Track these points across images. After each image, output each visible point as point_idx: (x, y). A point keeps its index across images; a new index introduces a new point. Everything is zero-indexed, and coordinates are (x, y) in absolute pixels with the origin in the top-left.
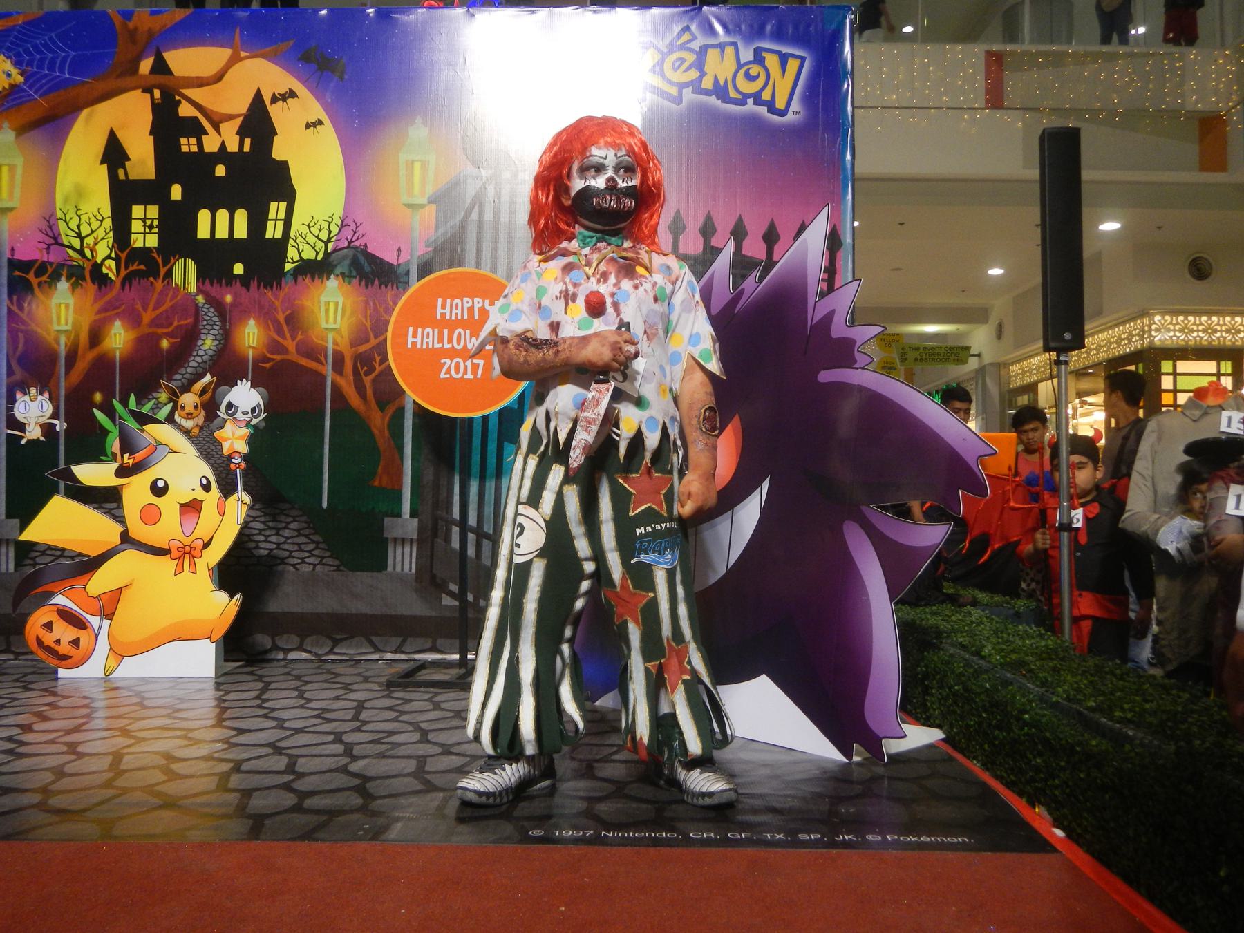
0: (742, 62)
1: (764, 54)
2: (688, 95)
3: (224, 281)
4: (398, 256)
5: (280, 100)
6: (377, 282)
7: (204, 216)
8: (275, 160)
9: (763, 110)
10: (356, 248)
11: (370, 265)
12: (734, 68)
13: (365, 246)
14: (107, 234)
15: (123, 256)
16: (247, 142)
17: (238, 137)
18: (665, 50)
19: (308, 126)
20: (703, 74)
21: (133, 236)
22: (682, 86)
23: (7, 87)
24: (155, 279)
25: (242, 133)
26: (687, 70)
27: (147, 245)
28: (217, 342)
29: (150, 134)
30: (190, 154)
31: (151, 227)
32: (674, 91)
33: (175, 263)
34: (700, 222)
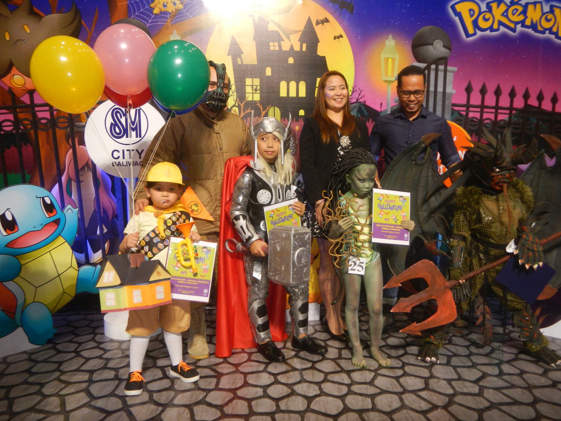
0: (545, 11)
1: (555, 9)
2: (519, 28)
3: (294, 120)
4: (381, 107)
5: (320, 23)
6: (371, 120)
7: (283, 85)
8: (318, 56)
9: (553, 37)
10: (360, 103)
11: (367, 111)
12: (540, 15)
13: (365, 102)
14: (233, 93)
15: (242, 105)
16: (304, 46)
17: (299, 43)
18: (509, 4)
19: (335, 38)
20: (526, 17)
21: (247, 95)
22: (516, 23)
23: (174, 11)
24: (259, 117)
25: (301, 41)
26: (519, 15)
27: (254, 100)
28: (292, 151)
29: (253, 40)
30: (275, 50)
31: (256, 90)
32: (512, 26)
33: (269, 109)
34: (523, 92)
